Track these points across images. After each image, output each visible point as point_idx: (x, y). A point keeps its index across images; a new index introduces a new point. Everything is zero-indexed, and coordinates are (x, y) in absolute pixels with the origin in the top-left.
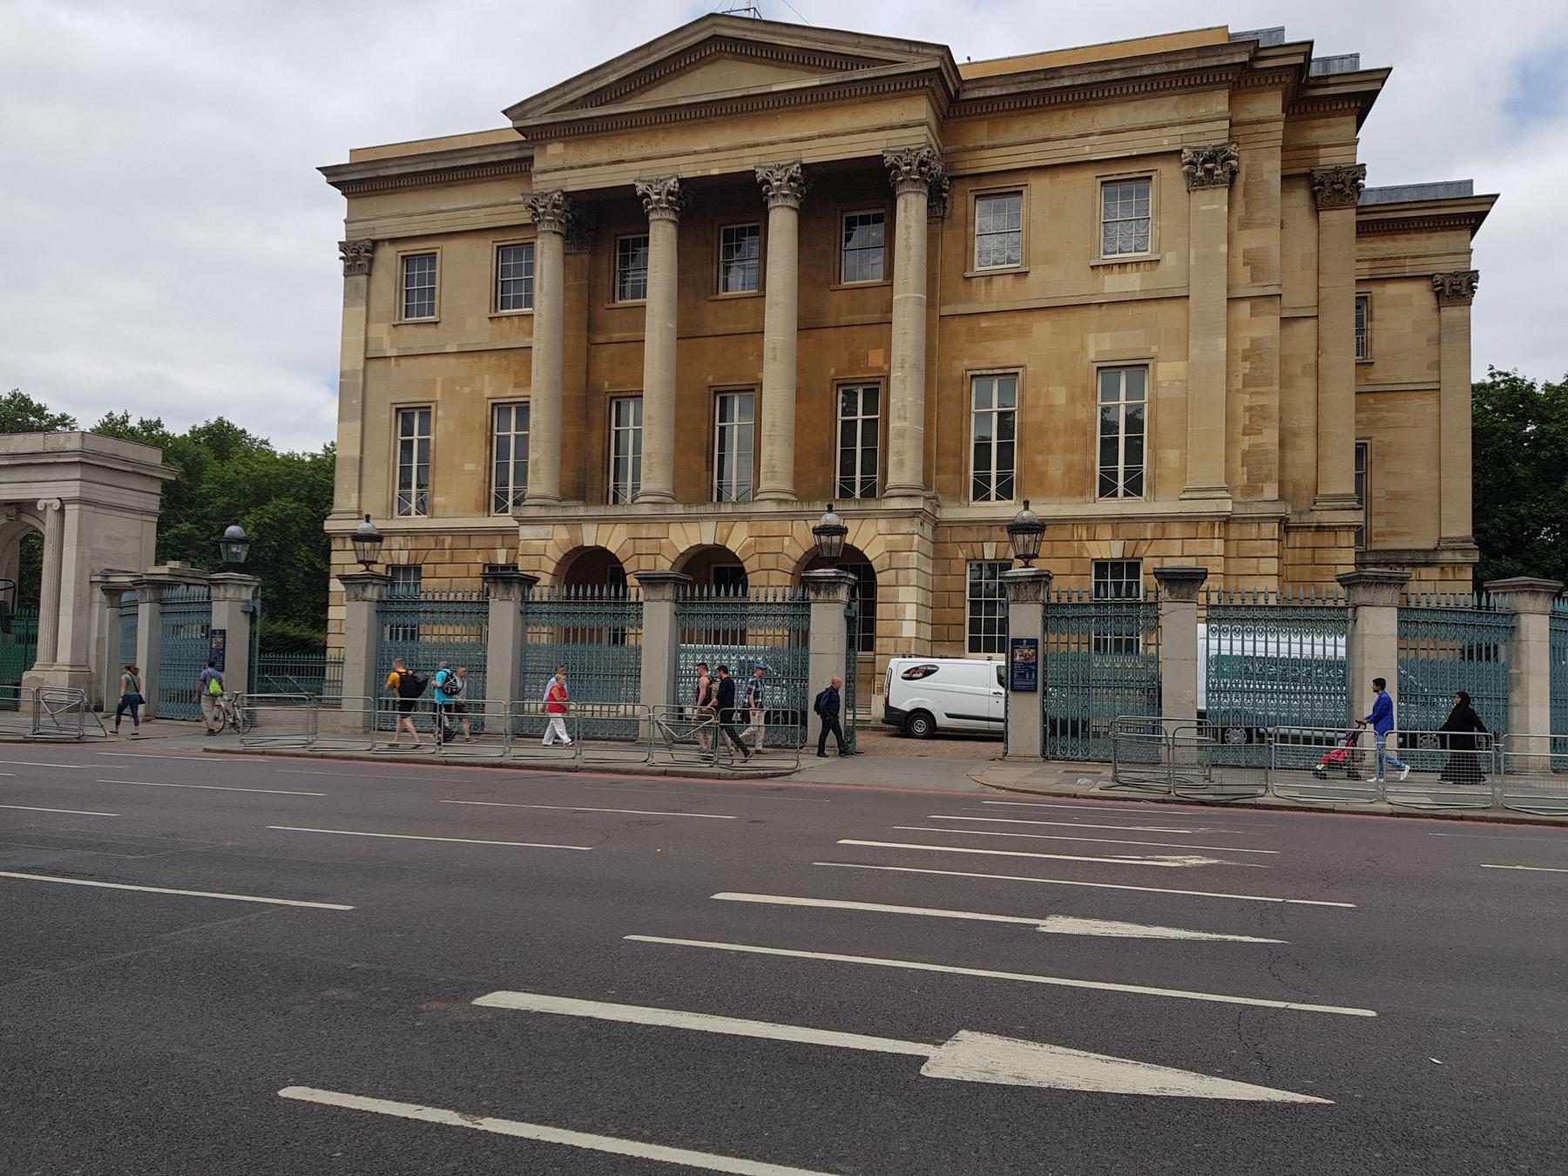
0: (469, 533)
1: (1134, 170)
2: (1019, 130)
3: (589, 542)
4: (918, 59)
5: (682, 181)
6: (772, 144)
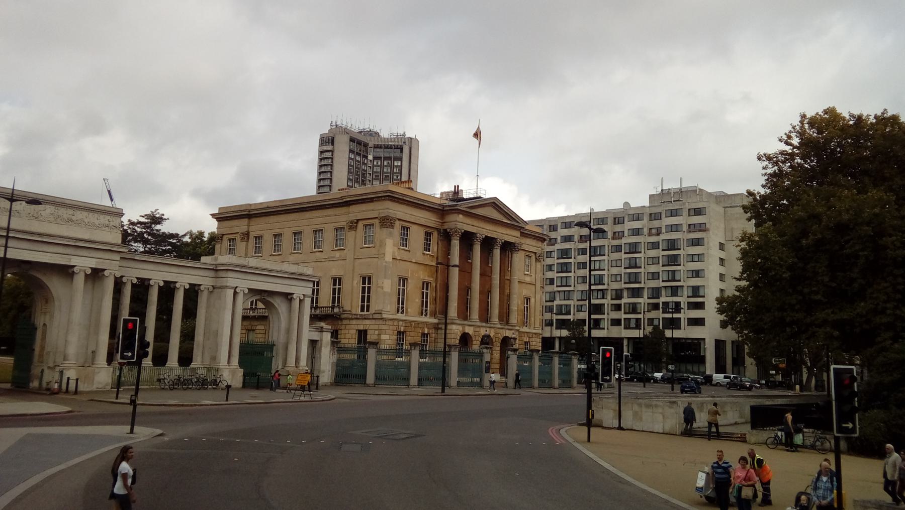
0: (418, 323)
3: (466, 332)
6: (499, 233)
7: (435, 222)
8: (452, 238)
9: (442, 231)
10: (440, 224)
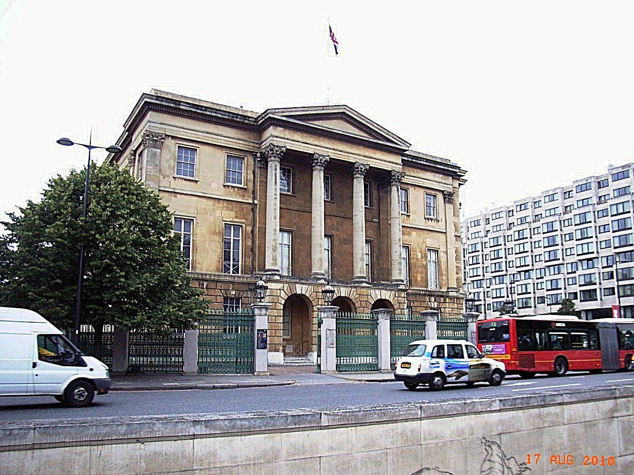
1: (433, 192)
3: (299, 292)
4: (404, 146)
7: (252, 144)
8: (269, 159)
9: (258, 155)
10: (257, 146)
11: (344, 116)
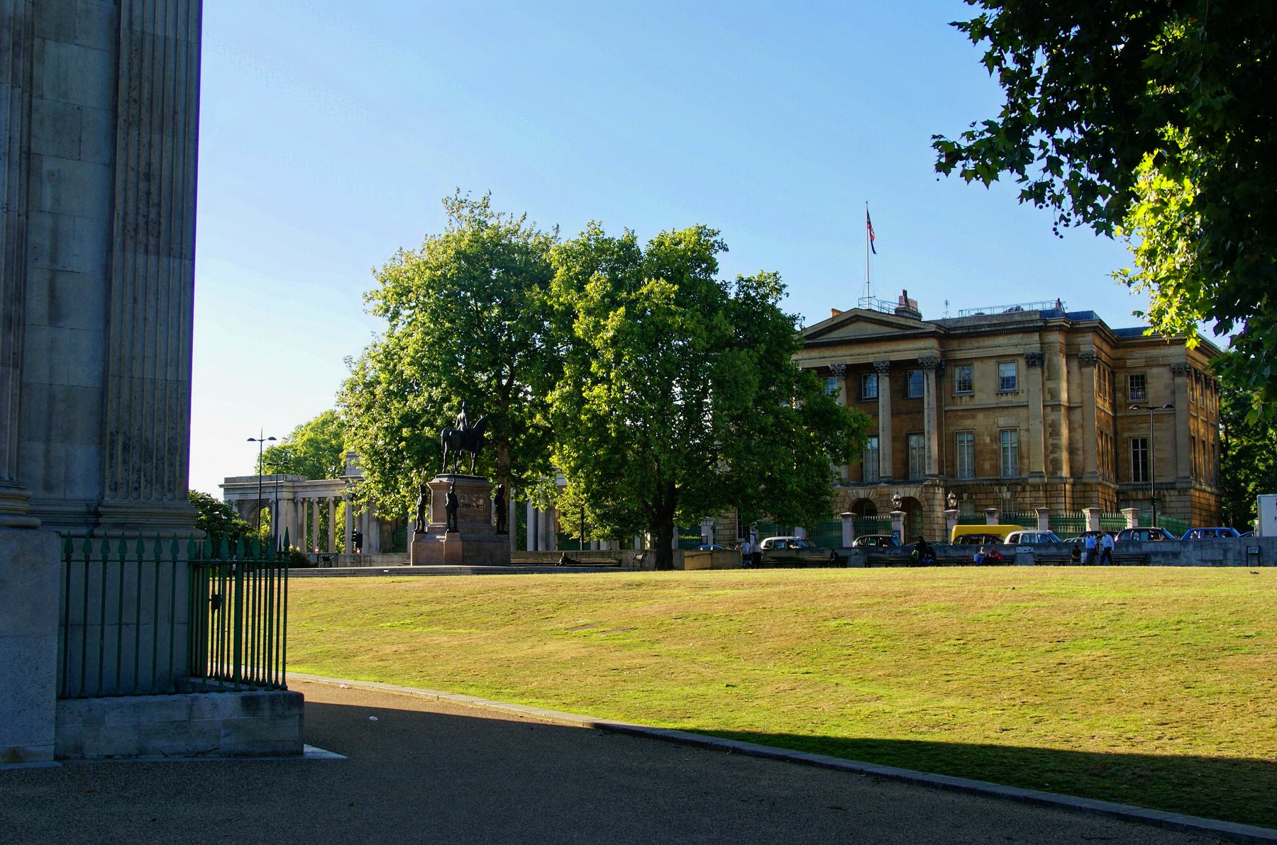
2: (969, 344)
5: (846, 365)
11: (856, 317)
